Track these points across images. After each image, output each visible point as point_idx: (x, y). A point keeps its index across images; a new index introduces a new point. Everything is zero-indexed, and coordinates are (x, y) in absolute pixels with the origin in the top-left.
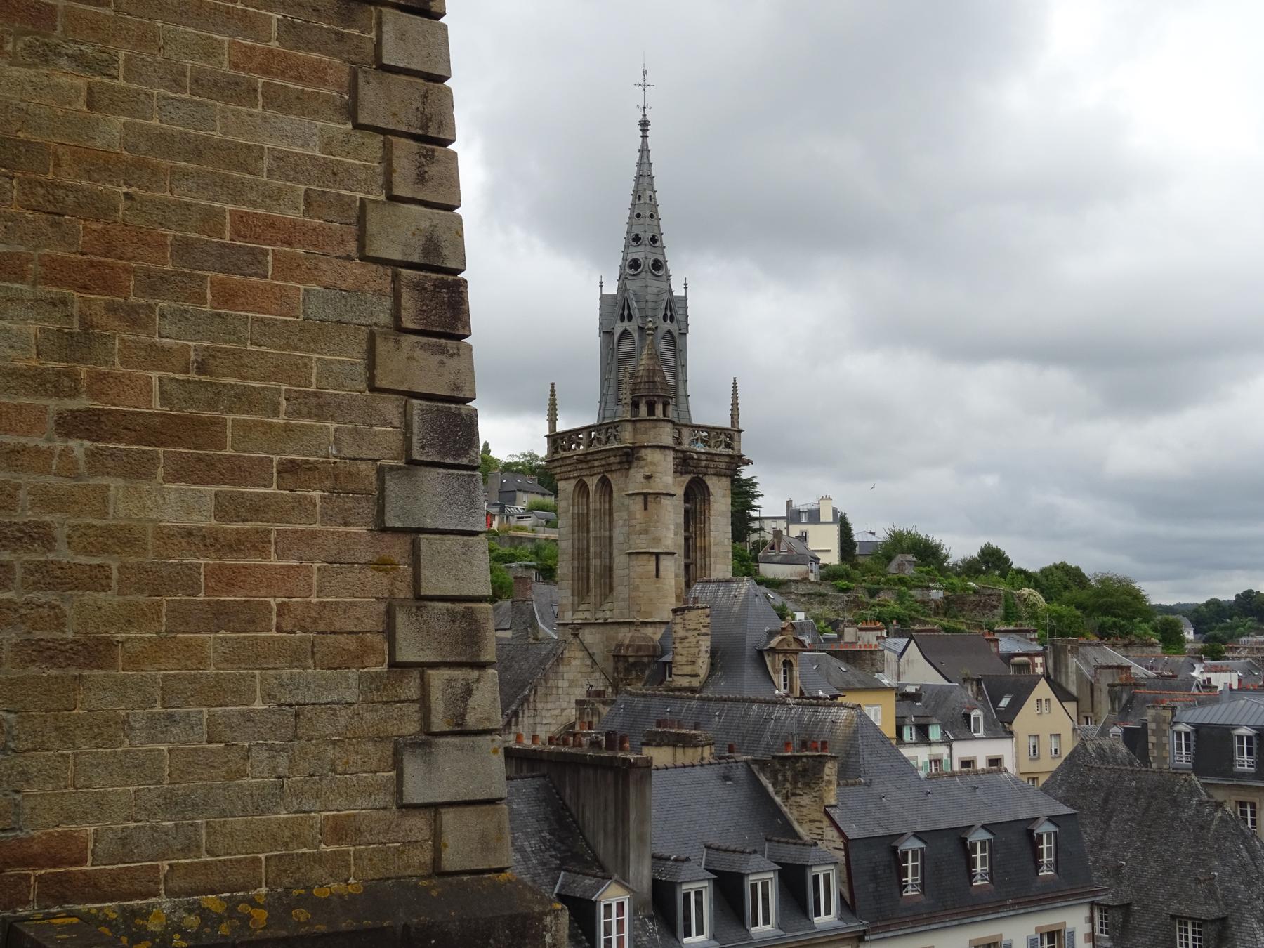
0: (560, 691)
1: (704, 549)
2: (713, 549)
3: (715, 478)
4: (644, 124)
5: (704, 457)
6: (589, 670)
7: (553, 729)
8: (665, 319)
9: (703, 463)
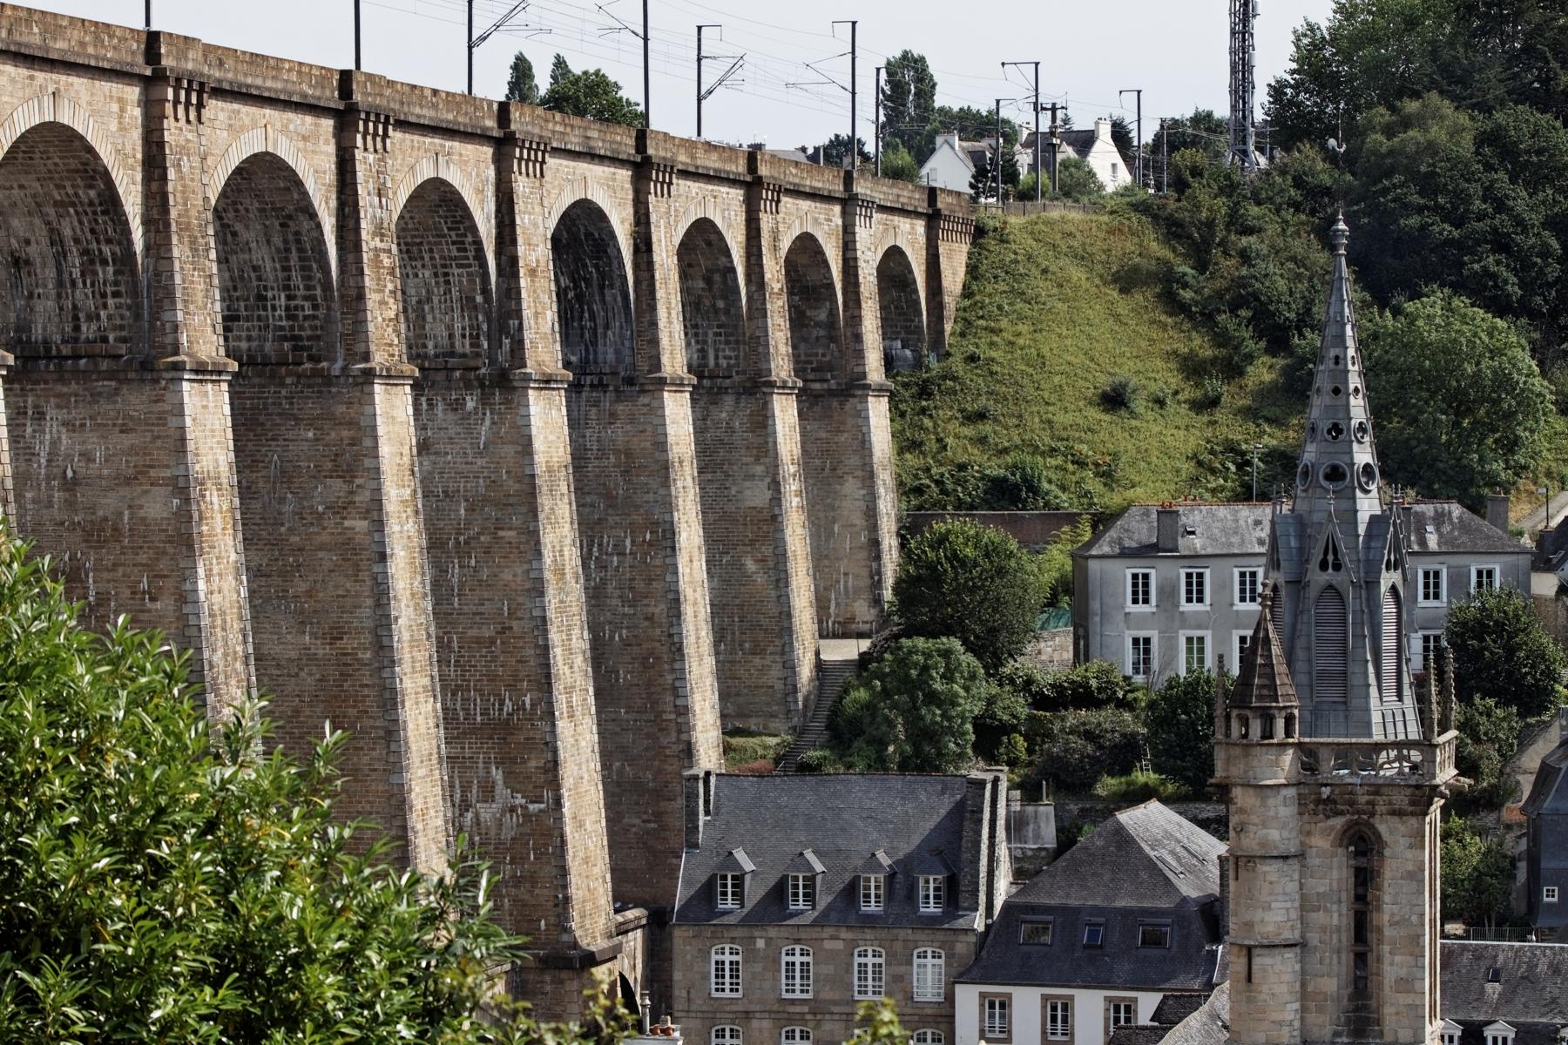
1: (1380, 930)
2: (1388, 932)
3: (1394, 821)
8: (1324, 566)
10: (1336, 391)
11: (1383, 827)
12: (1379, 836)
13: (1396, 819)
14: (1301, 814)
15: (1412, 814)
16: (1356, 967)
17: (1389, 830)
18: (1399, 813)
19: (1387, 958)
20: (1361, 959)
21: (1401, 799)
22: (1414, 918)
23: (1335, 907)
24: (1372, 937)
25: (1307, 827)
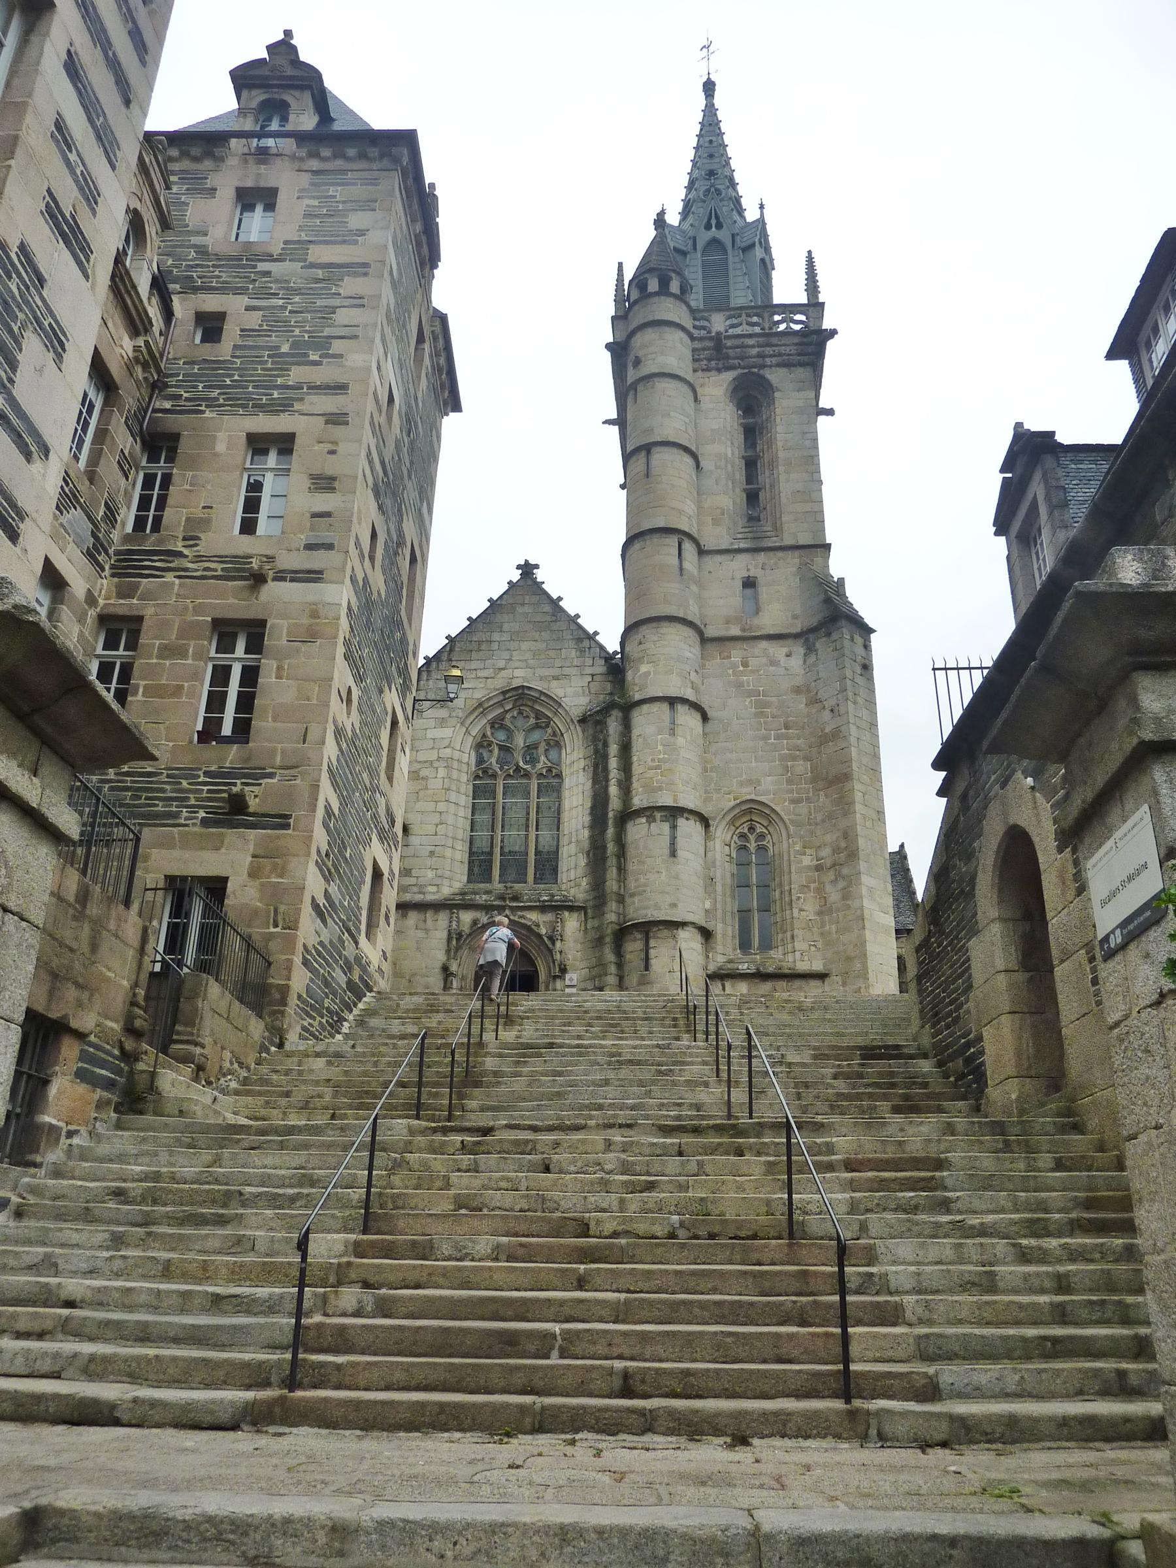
0: (495, 646)
1: (773, 464)
2: (782, 455)
3: (782, 371)
4: (709, 87)
5: (751, 342)
6: (548, 618)
7: (478, 695)
8: (708, 227)
9: (754, 351)
10: (711, 156)
11: (774, 376)
12: (767, 388)
14: (695, 371)
19: (782, 478)
20: (752, 497)
21: (789, 349)
22: (808, 443)
23: (729, 443)
24: (764, 478)
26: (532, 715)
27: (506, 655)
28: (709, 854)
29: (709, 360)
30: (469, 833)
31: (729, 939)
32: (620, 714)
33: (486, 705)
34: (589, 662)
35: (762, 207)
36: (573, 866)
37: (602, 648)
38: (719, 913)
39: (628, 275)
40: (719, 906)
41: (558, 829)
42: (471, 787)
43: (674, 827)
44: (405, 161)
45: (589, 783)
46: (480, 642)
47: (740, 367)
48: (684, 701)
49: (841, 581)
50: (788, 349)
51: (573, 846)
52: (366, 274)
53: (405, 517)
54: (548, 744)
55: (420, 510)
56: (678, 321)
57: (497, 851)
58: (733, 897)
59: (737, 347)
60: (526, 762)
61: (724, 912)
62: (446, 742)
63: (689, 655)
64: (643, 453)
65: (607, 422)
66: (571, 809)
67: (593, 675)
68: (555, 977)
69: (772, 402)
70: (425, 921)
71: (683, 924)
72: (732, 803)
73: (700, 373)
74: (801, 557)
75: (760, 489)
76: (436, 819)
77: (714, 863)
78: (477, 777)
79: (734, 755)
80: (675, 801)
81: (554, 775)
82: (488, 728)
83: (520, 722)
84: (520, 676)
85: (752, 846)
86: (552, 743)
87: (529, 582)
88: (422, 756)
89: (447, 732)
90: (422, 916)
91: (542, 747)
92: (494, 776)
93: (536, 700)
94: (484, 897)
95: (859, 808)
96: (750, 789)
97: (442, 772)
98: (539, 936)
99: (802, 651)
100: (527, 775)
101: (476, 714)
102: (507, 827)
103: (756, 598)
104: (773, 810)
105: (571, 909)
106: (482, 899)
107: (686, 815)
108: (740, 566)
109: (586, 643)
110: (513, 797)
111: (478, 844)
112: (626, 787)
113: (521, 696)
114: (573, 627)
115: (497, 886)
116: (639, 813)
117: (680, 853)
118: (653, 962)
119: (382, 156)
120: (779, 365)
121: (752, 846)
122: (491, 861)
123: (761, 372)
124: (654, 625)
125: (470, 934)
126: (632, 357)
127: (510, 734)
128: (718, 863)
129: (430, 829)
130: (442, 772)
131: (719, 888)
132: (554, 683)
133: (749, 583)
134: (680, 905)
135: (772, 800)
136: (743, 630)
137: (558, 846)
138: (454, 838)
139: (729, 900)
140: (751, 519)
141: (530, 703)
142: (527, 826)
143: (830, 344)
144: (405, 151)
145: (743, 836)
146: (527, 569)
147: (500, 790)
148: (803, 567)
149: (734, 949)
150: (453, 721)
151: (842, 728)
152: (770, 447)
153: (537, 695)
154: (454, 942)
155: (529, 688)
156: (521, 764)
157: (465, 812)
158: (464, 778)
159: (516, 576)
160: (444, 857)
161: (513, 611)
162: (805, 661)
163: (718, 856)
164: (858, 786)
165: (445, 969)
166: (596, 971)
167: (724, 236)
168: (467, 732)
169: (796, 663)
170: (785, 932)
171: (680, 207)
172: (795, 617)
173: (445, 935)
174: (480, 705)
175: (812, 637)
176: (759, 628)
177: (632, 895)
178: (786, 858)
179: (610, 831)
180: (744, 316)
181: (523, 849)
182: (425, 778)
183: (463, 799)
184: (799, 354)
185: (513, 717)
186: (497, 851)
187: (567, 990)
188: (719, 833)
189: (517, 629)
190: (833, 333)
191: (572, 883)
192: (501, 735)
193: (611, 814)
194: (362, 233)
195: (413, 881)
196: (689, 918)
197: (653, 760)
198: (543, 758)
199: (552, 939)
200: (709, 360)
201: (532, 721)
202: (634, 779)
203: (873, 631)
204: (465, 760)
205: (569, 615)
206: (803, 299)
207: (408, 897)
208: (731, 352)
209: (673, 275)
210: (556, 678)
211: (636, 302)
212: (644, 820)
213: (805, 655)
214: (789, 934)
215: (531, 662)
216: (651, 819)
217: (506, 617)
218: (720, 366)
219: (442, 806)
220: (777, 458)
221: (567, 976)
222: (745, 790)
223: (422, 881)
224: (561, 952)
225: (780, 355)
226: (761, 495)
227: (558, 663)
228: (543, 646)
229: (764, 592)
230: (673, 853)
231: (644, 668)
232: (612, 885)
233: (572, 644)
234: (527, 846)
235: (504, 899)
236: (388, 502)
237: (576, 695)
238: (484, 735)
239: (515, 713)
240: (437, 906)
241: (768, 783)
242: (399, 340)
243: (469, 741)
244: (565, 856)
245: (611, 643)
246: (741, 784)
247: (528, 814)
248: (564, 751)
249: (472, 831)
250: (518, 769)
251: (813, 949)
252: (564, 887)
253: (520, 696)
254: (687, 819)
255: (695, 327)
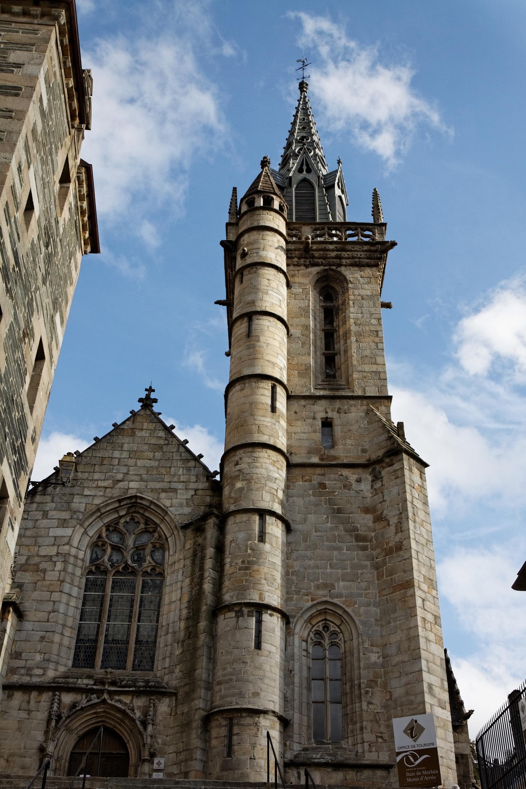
1: (347, 335)
5: (331, 247)
7: (97, 501)
8: (300, 170)
9: (333, 254)
13: (357, 269)
15: (369, 266)
16: (326, 368)
17: (352, 275)
18: (360, 265)
22: (374, 321)
25: (293, 272)
26: (142, 521)
27: (124, 470)
28: (289, 648)
29: (299, 258)
30: (78, 622)
31: (304, 729)
32: (217, 521)
33: (103, 511)
34: (193, 479)
35: (339, 162)
36: (168, 654)
37: (205, 468)
38: (296, 703)
39: (240, 195)
40: (296, 697)
41: (157, 621)
42: (84, 581)
43: (259, 622)
44: (63, 20)
45: (187, 581)
46: (103, 458)
47: (322, 264)
48: (273, 514)
49: (401, 425)
50: (359, 253)
51: (170, 637)
52: (17, 95)
53: (35, 313)
54: (154, 546)
55: (52, 317)
56: (276, 227)
57: (102, 638)
58: (309, 689)
59: (320, 250)
60: (134, 561)
61: (301, 703)
62: (66, 540)
63: (276, 475)
64: (246, 319)
65: (218, 302)
66: (171, 603)
67: (196, 490)
68: (144, 761)
69: (346, 290)
70: (29, 702)
71: (265, 712)
72: (310, 604)
73: (292, 267)
74: (368, 405)
75: (337, 354)
76: (49, 607)
77: (293, 656)
78: (90, 572)
79: (312, 563)
80: (261, 598)
81: (158, 573)
82: (104, 529)
83: (131, 527)
84: (134, 486)
85: (326, 643)
86: (157, 545)
87: (148, 412)
88: (43, 551)
89: (68, 532)
90: (26, 697)
91: (149, 548)
92: (105, 572)
93: (146, 508)
94: (86, 681)
95: (420, 612)
96: (325, 592)
97: (59, 566)
98: (134, 720)
99: (370, 478)
100: (134, 573)
101: (94, 517)
102: (112, 617)
103: (332, 435)
104: (345, 611)
105: (164, 694)
106: (83, 682)
107: (269, 612)
108: (320, 410)
109: (192, 463)
110: (120, 590)
111: (85, 632)
112: (218, 584)
113: (134, 505)
114: (182, 449)
115: (98, 671)
116: (230, 607)
117: (264, 645)
118: (236, 748)
119: (43, 15)
120: (352, 265)
121: (326, 643)
122: (95, 648)
123: (339, 269)
124: (250, 449)
125: (69, 717)
126: (240, 252)
127: (123, 539)
128: (296, 657)
129: (42, 615)
130: (59, 566)
131: (297, 680)
132: (163, 495)
133: (327, 424)
134: (262, 694)
135: (344, 603)
136: (322, 459)
137: (156, 637)
138: (64, 625)
139: (305, 691)
140: (328, 376)
141: (141, 511)
142: (130, 617)
143: (390, 252)
144: (64, 13)
145: (318, 633)
146: (147, 402)
147: (109, 585)
148: (369, 412)
149: (309, 739)
150: (74, 522)
151: (405, 542)
152: (344, 322)
153: (148, 504)
154: (53, 723)
155: (142, 498)
156: (130, 562)
157: (75, 603)
158: (78, 572)
159: (137, 407)
160: (52, 642)
161: (133, 434)
162: (372, 486)
163: (296, 651)
164: (418, 593)
165: (42, 750)
166: (182, 757)
167: (311, 177)
168: (85, 533)
169: (365, 487)
170: (356, 723)
171: (280, 160)
172: (364, 451)
173: (46, 714)
174: (98, 510)
175: (378, 467)
176: (335, 458)
177: (220, 683)
178: (356, 655)
179: (203, 624)
180: (326, 229)
181: (125, 638)
182: (44, 571)
183: (75, 591)
184: (368, 258)
185: (126, 522)
186: (102, 638)
187: (155, 776)
188: (297, 630)
189: (135, 449)
190: (393, 244)
191: (167, 671)
192: (115, 538)
193: (204, 608)
194: (19, 66)
195: (21, 663)
196: (271, 706)
197: (243, 562)
198: (148, 558)
199: (144, 724)
200: (299, 258)
201: (142, 526)
202: (226, 579)
203: (426, 465)
204: (81, 555)
205: (179, 440)
206: (371, 220)
207: (15, 679)
208: (316, 254)
209: (274, 197)
210: (164, 490)
211: (246, 213)
212: (233, 614)
213: (373, 481)
214: (358, 725)
215: (144, 476)
216: (239, 614)
217: (126, 440)
218: (308, 263)
219: (56, 596)
220: (350, 330)
221: (156, 760)
222: (320, 592)
223: (30, 663)
224: (151, 736)
225: (353, 258)
226: (337, 358)
227: (167, 479)
228: (156, 464)
229: (338, 430)
230: (258, 646)
231: (239, 485)
232: (201, 673)
233: (179, 464)
234: (129, 635)
235: (103, 683)
236: (18, 291)
237: (181, 505)
238: (100, 537)
239: (128, 519)
240: (40, 689)
241: (341, 586)
242: (44, 162)
243: (86, 540)
244: (162, 645)
245: (214, 466)
246: (318, 587)
247: (132, 606)
248: (167, 553)
249: (81, 620)
250: (127, 566)
251: (380, 740)
252: (158, 675)
253: (134, 504)
254: (271, 615)
255: (288, 235)
